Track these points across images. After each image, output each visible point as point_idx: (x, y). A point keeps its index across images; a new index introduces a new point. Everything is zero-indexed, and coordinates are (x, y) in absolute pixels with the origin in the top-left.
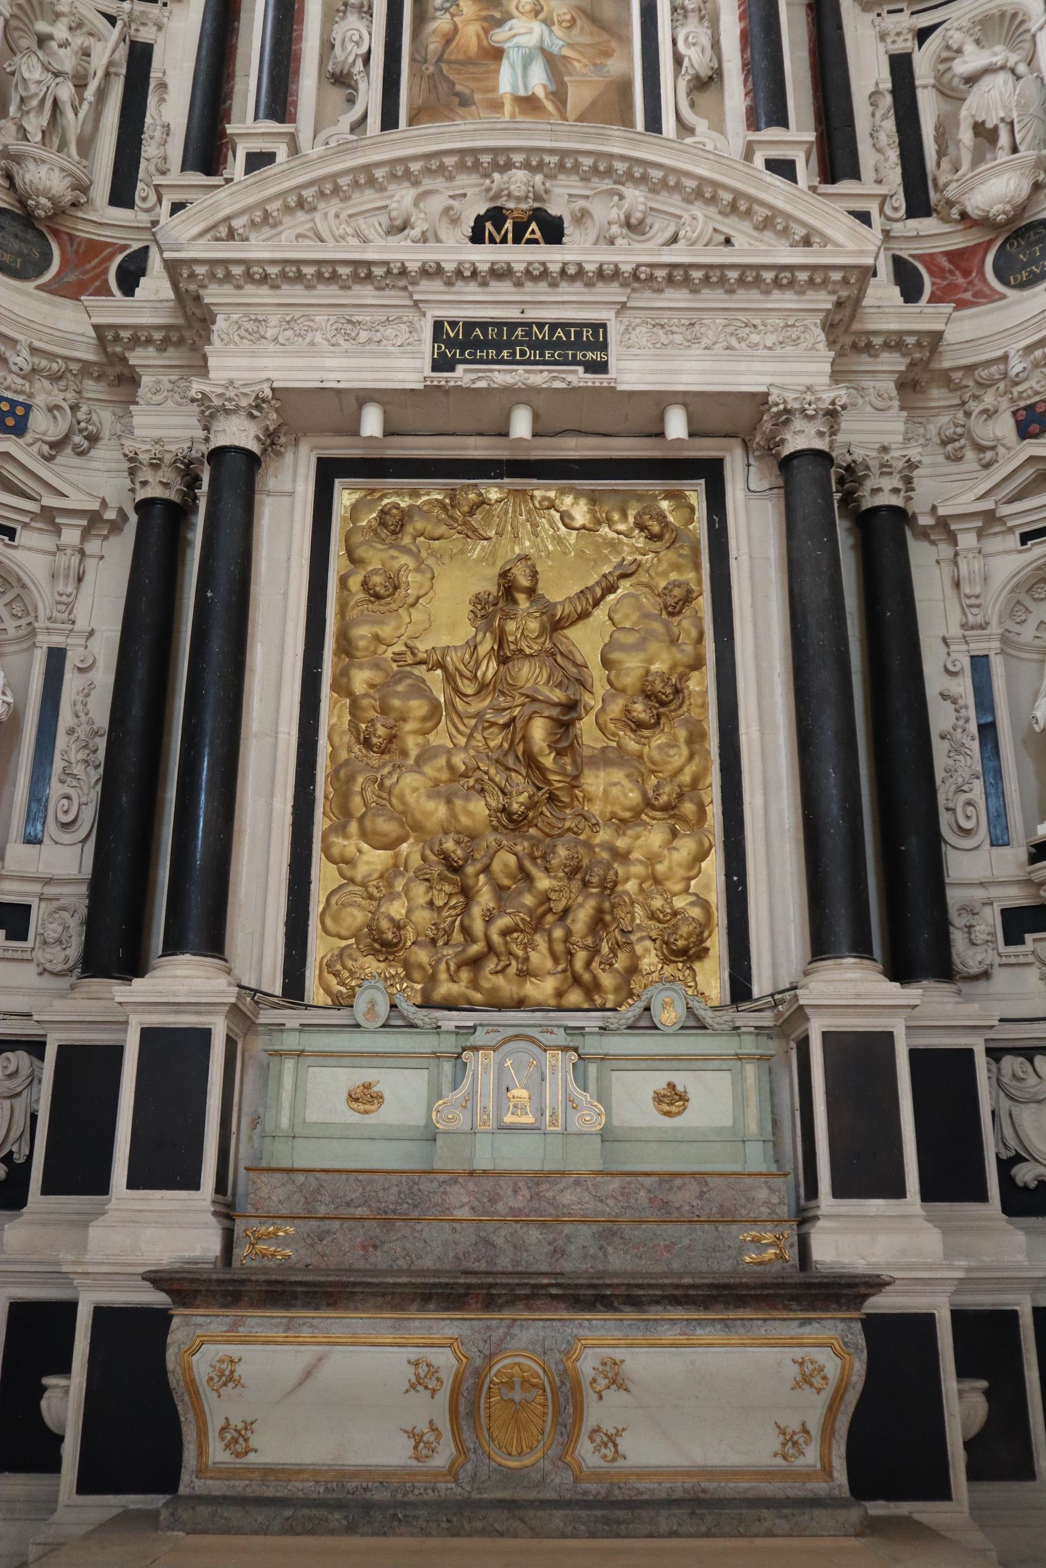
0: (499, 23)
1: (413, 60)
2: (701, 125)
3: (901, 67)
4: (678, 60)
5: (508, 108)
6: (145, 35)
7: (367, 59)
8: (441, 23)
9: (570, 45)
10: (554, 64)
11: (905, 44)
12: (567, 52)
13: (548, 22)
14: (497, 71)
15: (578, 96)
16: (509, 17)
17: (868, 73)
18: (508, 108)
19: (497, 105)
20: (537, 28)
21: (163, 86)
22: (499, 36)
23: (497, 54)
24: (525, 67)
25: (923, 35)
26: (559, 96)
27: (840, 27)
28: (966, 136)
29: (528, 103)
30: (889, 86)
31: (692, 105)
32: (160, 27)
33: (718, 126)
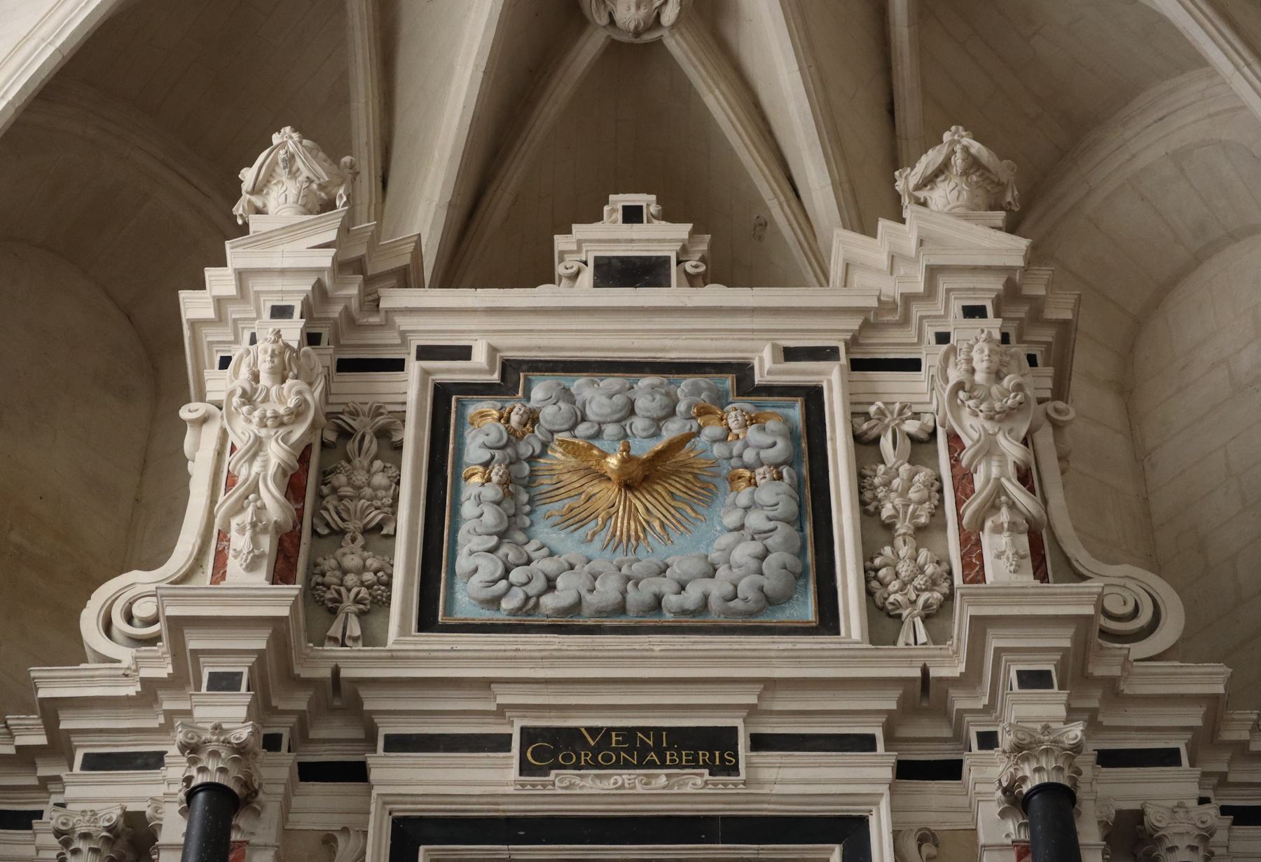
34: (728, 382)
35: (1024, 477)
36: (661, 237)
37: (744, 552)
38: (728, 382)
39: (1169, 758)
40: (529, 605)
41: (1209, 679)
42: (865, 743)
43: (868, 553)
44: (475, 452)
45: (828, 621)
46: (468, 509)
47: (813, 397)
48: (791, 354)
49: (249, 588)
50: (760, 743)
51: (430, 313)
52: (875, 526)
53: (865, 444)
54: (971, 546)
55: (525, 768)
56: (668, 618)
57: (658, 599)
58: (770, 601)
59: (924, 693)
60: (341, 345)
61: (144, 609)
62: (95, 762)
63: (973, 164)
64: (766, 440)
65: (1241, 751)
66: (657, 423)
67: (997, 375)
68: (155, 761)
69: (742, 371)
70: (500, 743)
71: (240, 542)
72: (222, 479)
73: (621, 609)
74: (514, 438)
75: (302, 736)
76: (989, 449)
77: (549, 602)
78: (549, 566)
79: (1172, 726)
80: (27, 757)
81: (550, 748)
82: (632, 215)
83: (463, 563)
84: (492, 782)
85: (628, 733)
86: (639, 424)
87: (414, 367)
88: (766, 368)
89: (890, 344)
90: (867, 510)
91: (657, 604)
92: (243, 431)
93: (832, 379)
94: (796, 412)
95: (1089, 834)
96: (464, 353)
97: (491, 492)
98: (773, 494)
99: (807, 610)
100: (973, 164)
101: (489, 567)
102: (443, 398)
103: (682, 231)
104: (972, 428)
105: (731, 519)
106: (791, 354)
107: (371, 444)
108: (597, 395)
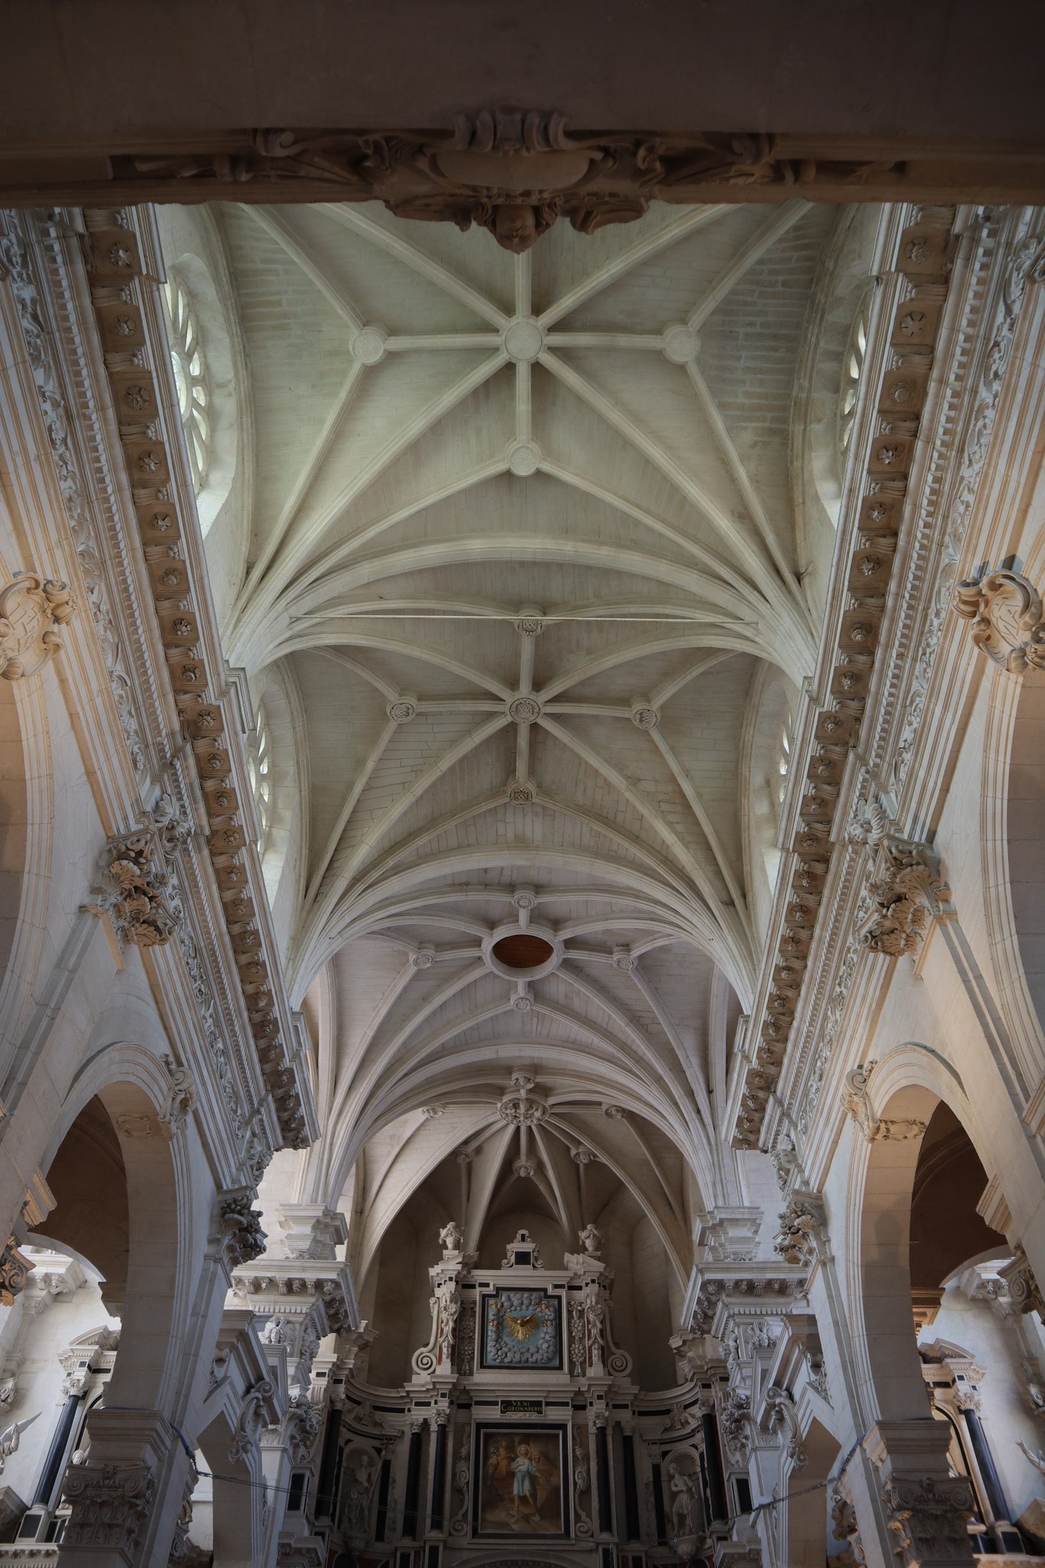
0: (513, 1460)
1: (483, 1478)
2: (583, 1515)
3: (656, 1469)
4: (575, 1483)
5: (516, 1502)
6: (388, 1457)
7: (468, 1483)
8: (493, 1460)
9: (538, 1471)
10: (533, 1479)
11: (657, 1460)
12: (538, 1475)
13: (530, 1459)
14: (513, 1484)
15: (541, 1495)
16: (517, 1457)
17: (644, 1475)
18: (516, 1502)
19: (512, 1500)
20: (527, 1461)
21: (394, 1481)
22: (514, 1465)
23: (512, 1475)
24: (523, 1482)
25: (665, 1454)
26: (534, 1495)
27: (633, 1462)
28: (675, 1520)
29: (523, 1499)
30: (651, 1479)
31: (580, 1502)
32: (393, 1452)
33: (589, 1516)
34: (542, 1294)
35: (602, 1336)
36: (528, 1247)
37: (545, 1346)
38: (542, 1294)
39: (626, 1406)
40: (502, 1361)
41: (635, 1390)
42: (566, 1404)
43: (570, 1346)
44: (491, 1317)
45: (560, 1367)
46: (490, 1333)
47: (559, 1298)
48: (556, 1286)
49: (445, 1369)
50: (548, 1404)
51: (481, 1275)
52: (571, 1340)
53: (570, 1312)
54: (590, 1348)
55: (502, 1412)
56: (530, 1365)
57: (527, 1361)
58: (550, 1360)
59: (579, 1393)
60: (464, 1284)
61: (425, 1361)
62: (418, 1404)
63: (594, 1236)
64: (549, 1314)
65: (642, 1400)
66: (528, 1307)
67: (597, 1303)
68: (428, 1404)
69: (545, 1290)
70: (495, 1403)
71: (445, 1350)
72: (440, 1322)
73: (520, 1362)
74: (499, 1311)
75: (458, 1398)
76: (595, 1325)
77: (506, 1360)
78: (505, 1349)
79: (627, 1400)
80: (402, 1397)
81: (507, 1406)
82: (523, 1258)
83: (489, 1349)
84: (494, 1414)
85: (522, 1402)
86: (524, 1307)
87: (478, 1290)
88: (551, 1291)
89: (576, 1283)
90: (570, 1332)
91: (527, 1361)
92: (444, 1316)
93: (563, 1293)
94: (556, 1303)
95: (609, 1431)
96: (487, 1285)
97: (494, 1329)
98: (550, 1330)
99: (556, 1363)
100: (594, 1236)
101: (494, 1351)
102: (484, 1297)
103: (533, 1246)
104: (591, 1317)
105: (542, 1335)
106: (556, 1286)
107: (470, 1313)
108: (515, 1298)
